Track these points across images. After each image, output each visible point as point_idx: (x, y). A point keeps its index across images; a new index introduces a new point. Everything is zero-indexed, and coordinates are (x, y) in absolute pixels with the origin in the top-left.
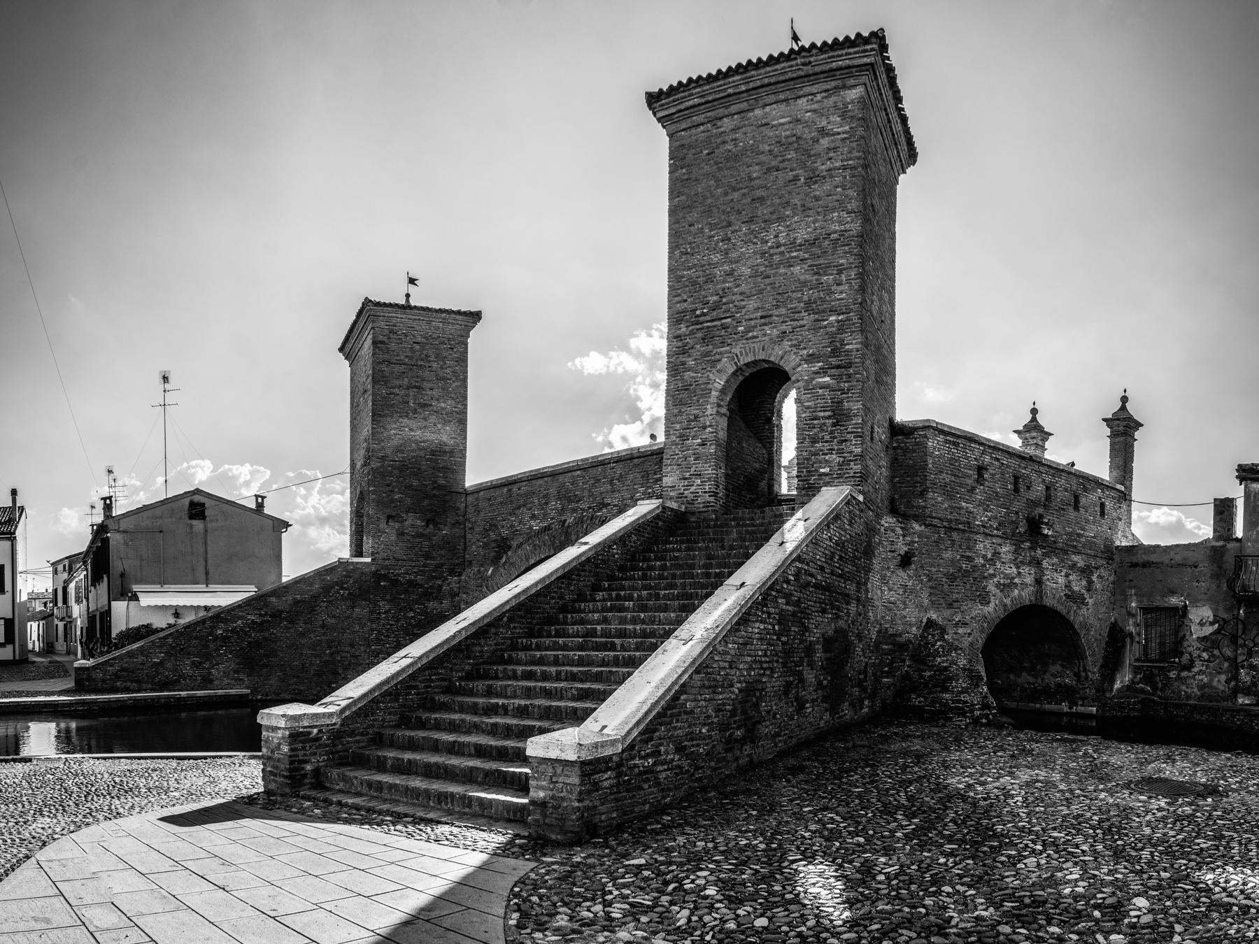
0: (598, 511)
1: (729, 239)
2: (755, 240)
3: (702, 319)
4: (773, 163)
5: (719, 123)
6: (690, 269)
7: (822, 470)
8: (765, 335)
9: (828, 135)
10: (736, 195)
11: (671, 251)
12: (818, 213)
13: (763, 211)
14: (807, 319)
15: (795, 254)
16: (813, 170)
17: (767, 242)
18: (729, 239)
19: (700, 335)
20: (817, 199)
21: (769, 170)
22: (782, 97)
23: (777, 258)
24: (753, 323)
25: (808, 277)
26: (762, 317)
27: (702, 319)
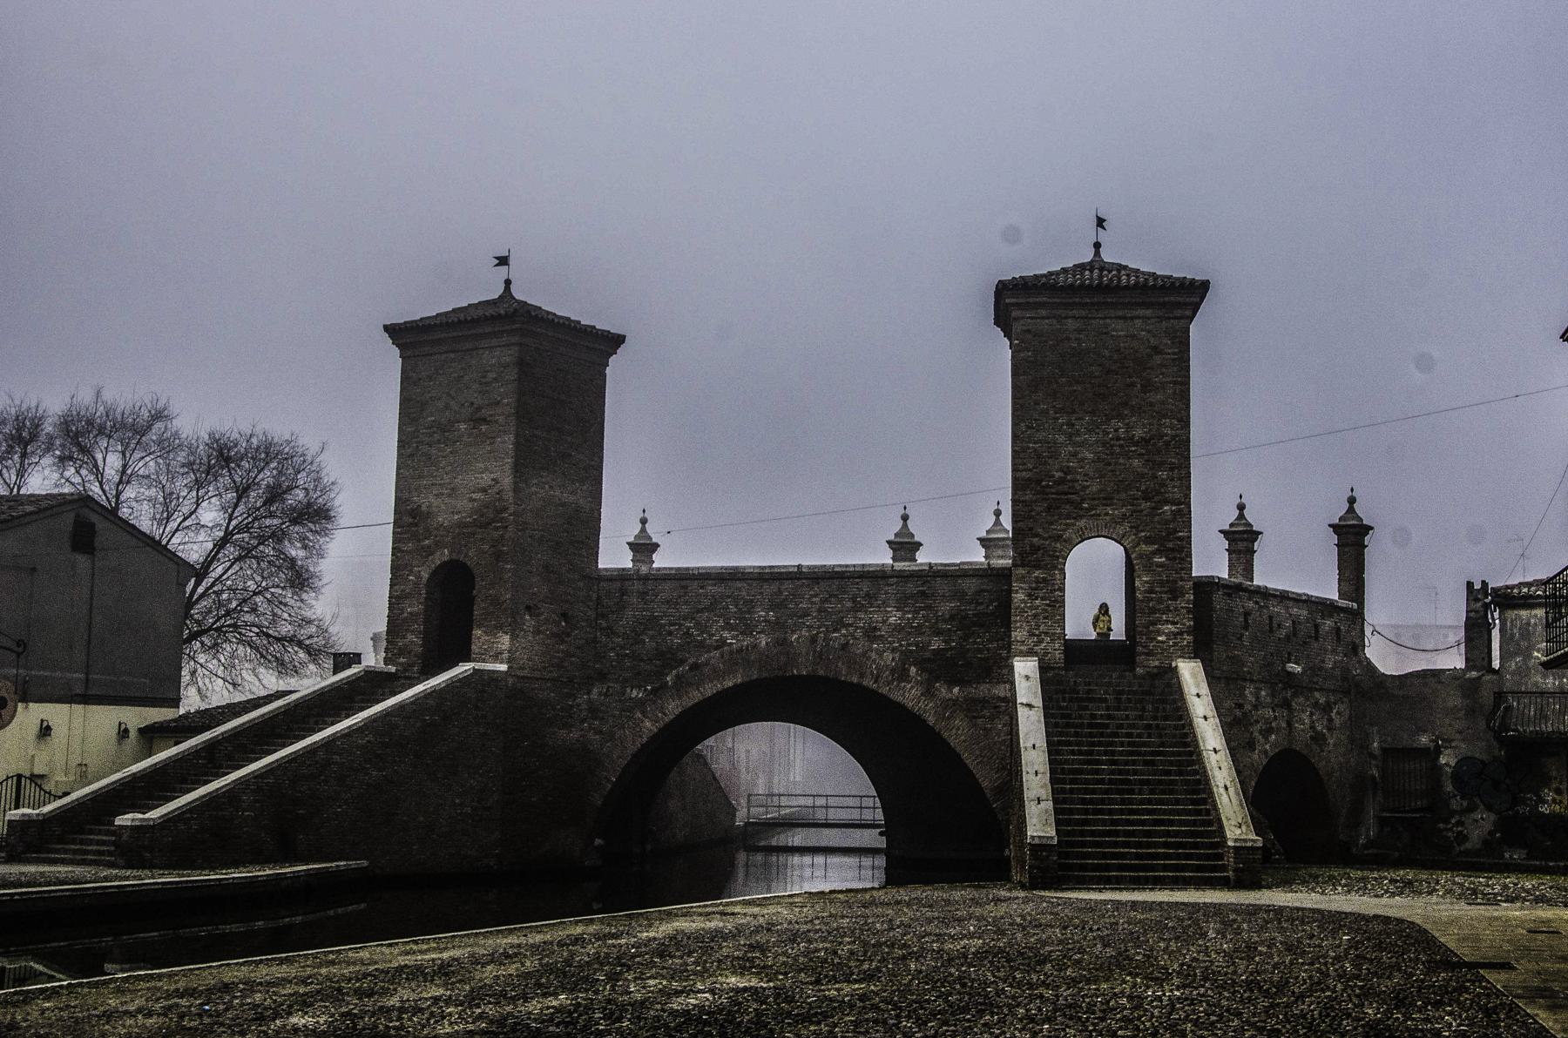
0: (835, 630)
1: (1073, 425)
2: (1097, 431)
7: (1160, 638)
8: (1107, 514)
9: (1160, 353)
11: (1014, 425)
12: (1153, 417)
14: (1145, 505)
15: (1133, 449)
17: (1108, 433)
18: (1073, 425)
20: (1151, 404)
21: (1109, 372)
22: (1120, 313)
25: (1146, 471)
26: (1105, 499)
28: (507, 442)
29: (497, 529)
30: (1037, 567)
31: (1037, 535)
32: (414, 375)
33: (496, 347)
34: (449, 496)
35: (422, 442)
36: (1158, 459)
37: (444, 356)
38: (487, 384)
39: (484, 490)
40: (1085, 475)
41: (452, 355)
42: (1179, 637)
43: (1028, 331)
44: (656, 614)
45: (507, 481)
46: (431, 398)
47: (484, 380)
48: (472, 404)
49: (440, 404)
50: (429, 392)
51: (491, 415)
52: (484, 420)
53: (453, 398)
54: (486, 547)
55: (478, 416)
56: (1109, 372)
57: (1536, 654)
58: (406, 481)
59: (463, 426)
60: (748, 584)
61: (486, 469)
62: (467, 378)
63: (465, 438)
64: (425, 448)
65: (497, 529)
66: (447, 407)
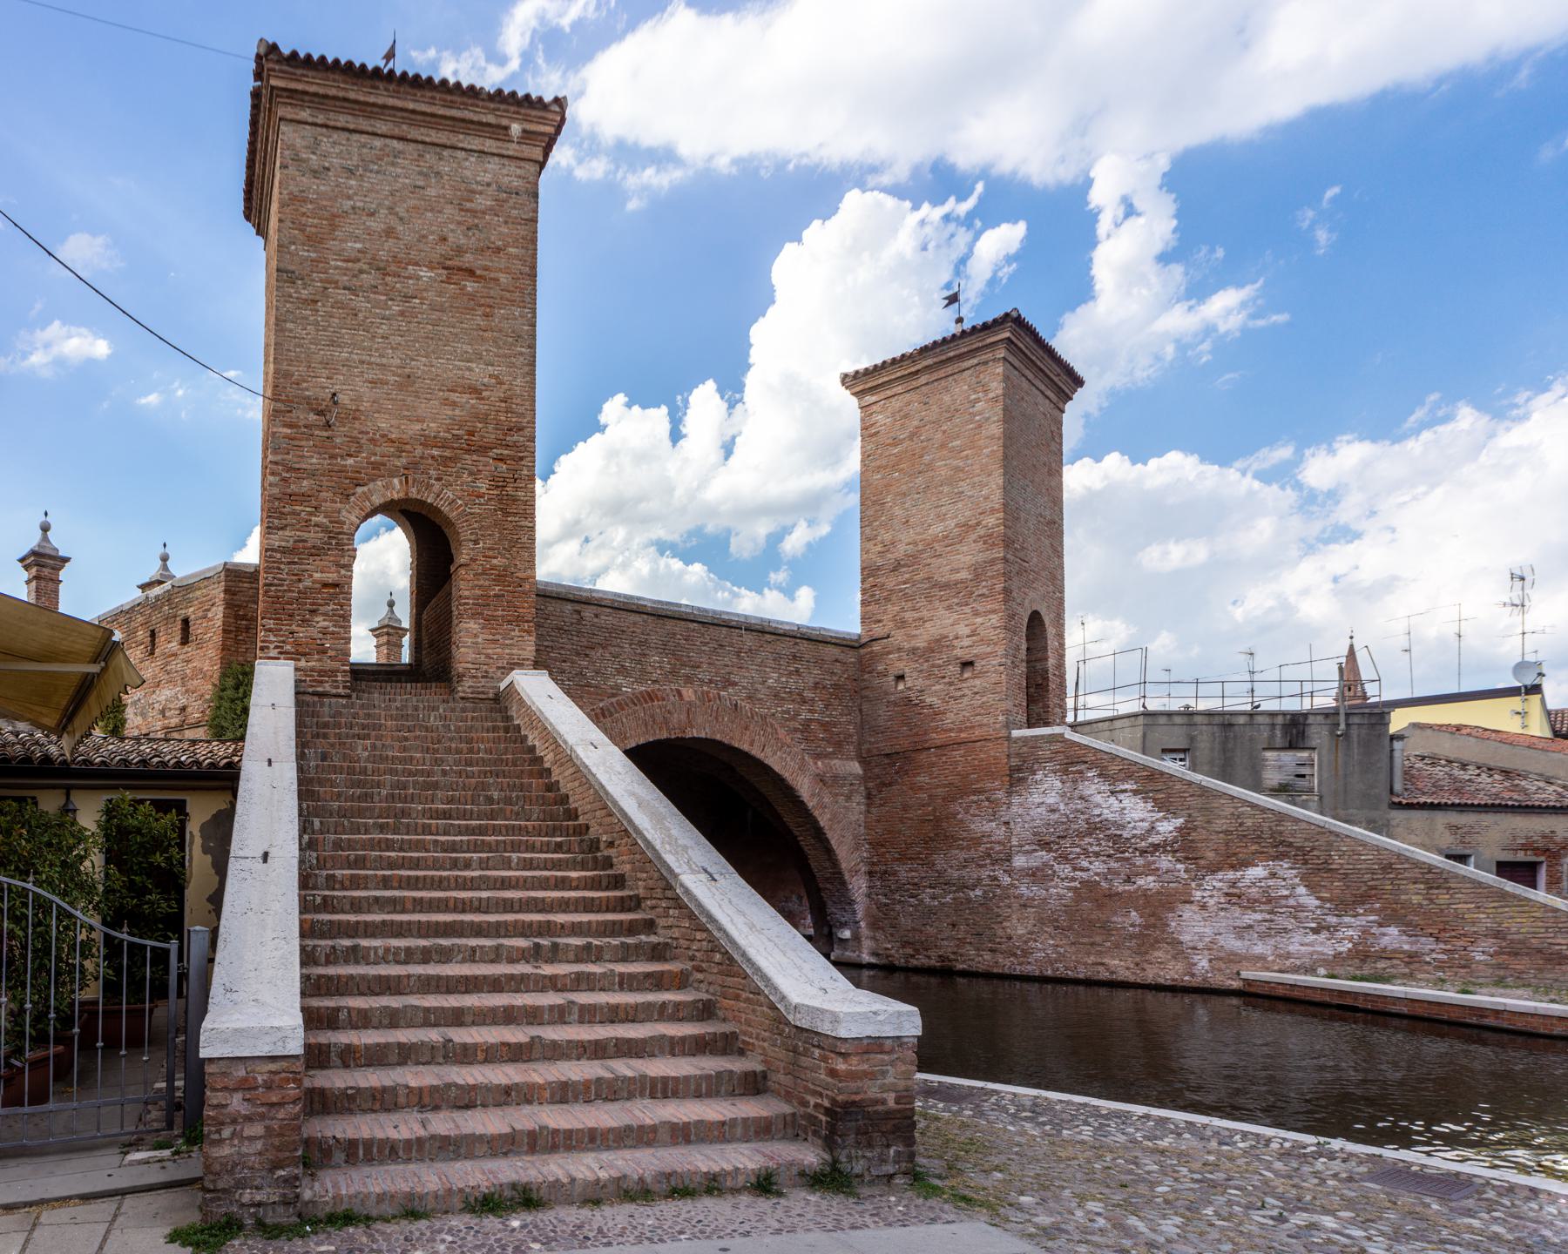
29: (500, 459)
32: (314, 157)
33: (493, 154)
34: (400, 387)
35: (337, 282)
37: (378, 143)
38: (473, 212)
41: (395, 143)
46: (353, 208)
47: (468, 205)
48: (444, 239)
49: (376, 225)
50: (349, 198)
51: (486, 269)
52: (471, 272)
53: (401, 219)
54: (483, 486)
59: (425, 274)
62: (431, 192)
63: (431, 295)
64: (343, 296)
65: (500, 459)
66: (389, 232)
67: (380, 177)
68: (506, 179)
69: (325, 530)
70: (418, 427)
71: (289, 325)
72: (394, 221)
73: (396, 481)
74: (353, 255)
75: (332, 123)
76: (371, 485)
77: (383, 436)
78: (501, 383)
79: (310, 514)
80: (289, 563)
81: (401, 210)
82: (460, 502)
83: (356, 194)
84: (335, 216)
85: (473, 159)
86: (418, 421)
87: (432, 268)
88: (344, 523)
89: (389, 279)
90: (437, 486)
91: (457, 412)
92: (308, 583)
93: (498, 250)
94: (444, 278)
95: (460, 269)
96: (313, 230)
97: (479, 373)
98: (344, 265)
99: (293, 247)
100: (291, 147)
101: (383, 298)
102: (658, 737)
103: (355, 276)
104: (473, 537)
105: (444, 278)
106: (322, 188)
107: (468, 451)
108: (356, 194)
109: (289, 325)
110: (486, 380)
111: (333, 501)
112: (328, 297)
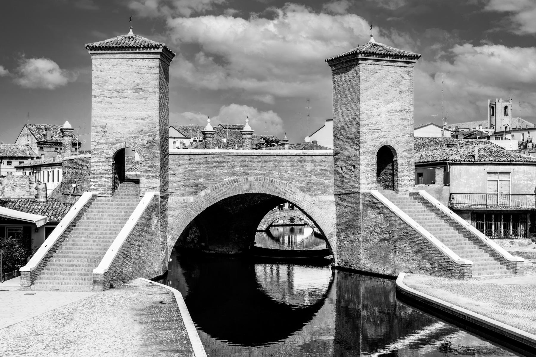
0: (268, 175)
1: (378, 104)
3: (371, 128)
4: (391, 84)
5: (375, 66)
6: (367, 111)
7: (406, 182)
8: (389, 137)
10: (380, 91)
13: (388, 98)
14: (400, 135)
15: (397, 114)
16: (401, 89)
19: (371, 133)
20: (402, 98)
21: (389, 85)
23: (392, 114)
24: (386, 133)
25: (401, 122)
26: (388, 132)
27: (371, 128)
28: (155, 99)
29: (151, 136)
30: (368, 156)
31: (368, 144)
34: (123, 120)
36: (404, 117)
37: (116, 60)
39: (143, 119)
40: (383, 123)
42: (410, 181)
43: (364, 69)
44: (194, 168)
45: (155, 115)
49: (116, 81)
50: (109, 75)
51: (145, 88)
54: (145, 143)
55: (137, 87)
56: (389, 85)
57: (462, 180)
58: (98, 113)
59: (129, 91)
60: (233, 157)
61: (144, 110)
62: (130, 71)
63: (131, 96)
64: (108, 99)
65: (151, 136)
66: (120, 82)
67: (117, 69)
68: (150, 64)
69: (105, 157)
70: (128, 130)
71: (95, 108)
72: (121, 79)
73: (122, 144)
74: (110, 89)
75: (104, 58)
76: (116, 145)
77: (119, 133)
78: (150, 116)
79: (102, 153)
80: (97, 165)
81: (122, 76)
82: (139, 147)
83: (111, 74)
84: (106, 80)
85: (141, 60)
86: (128, 128)
87: (131, 89)
88: (110, 155)
89: (120, 94)
90: (133, 144)
91: (138, 125)
92: (101, 170)
93: (149, 82)
94: (134, 92)
95: (138, 89)
96: (101, 84)
97: (144, 115)
98: (109, 92)
99: (96, 89)
100: (95, 65)
101: (118, 99)
102: (238, 194)
103: (111, 94)
104: (143, 156)
105: (134, 92)
106: (103, 74)
107: (141, 134)
108: (111, 74)
109: (95, 108)
110: (146, 116)
111: (107, 150)
112: (104, 100)
